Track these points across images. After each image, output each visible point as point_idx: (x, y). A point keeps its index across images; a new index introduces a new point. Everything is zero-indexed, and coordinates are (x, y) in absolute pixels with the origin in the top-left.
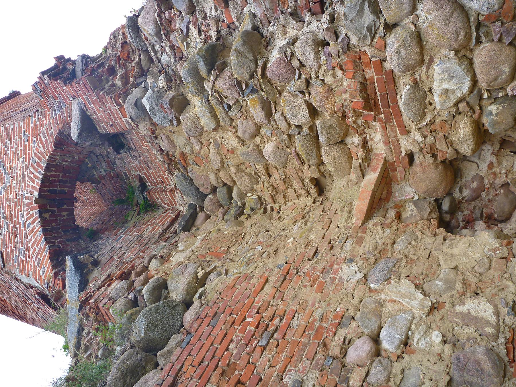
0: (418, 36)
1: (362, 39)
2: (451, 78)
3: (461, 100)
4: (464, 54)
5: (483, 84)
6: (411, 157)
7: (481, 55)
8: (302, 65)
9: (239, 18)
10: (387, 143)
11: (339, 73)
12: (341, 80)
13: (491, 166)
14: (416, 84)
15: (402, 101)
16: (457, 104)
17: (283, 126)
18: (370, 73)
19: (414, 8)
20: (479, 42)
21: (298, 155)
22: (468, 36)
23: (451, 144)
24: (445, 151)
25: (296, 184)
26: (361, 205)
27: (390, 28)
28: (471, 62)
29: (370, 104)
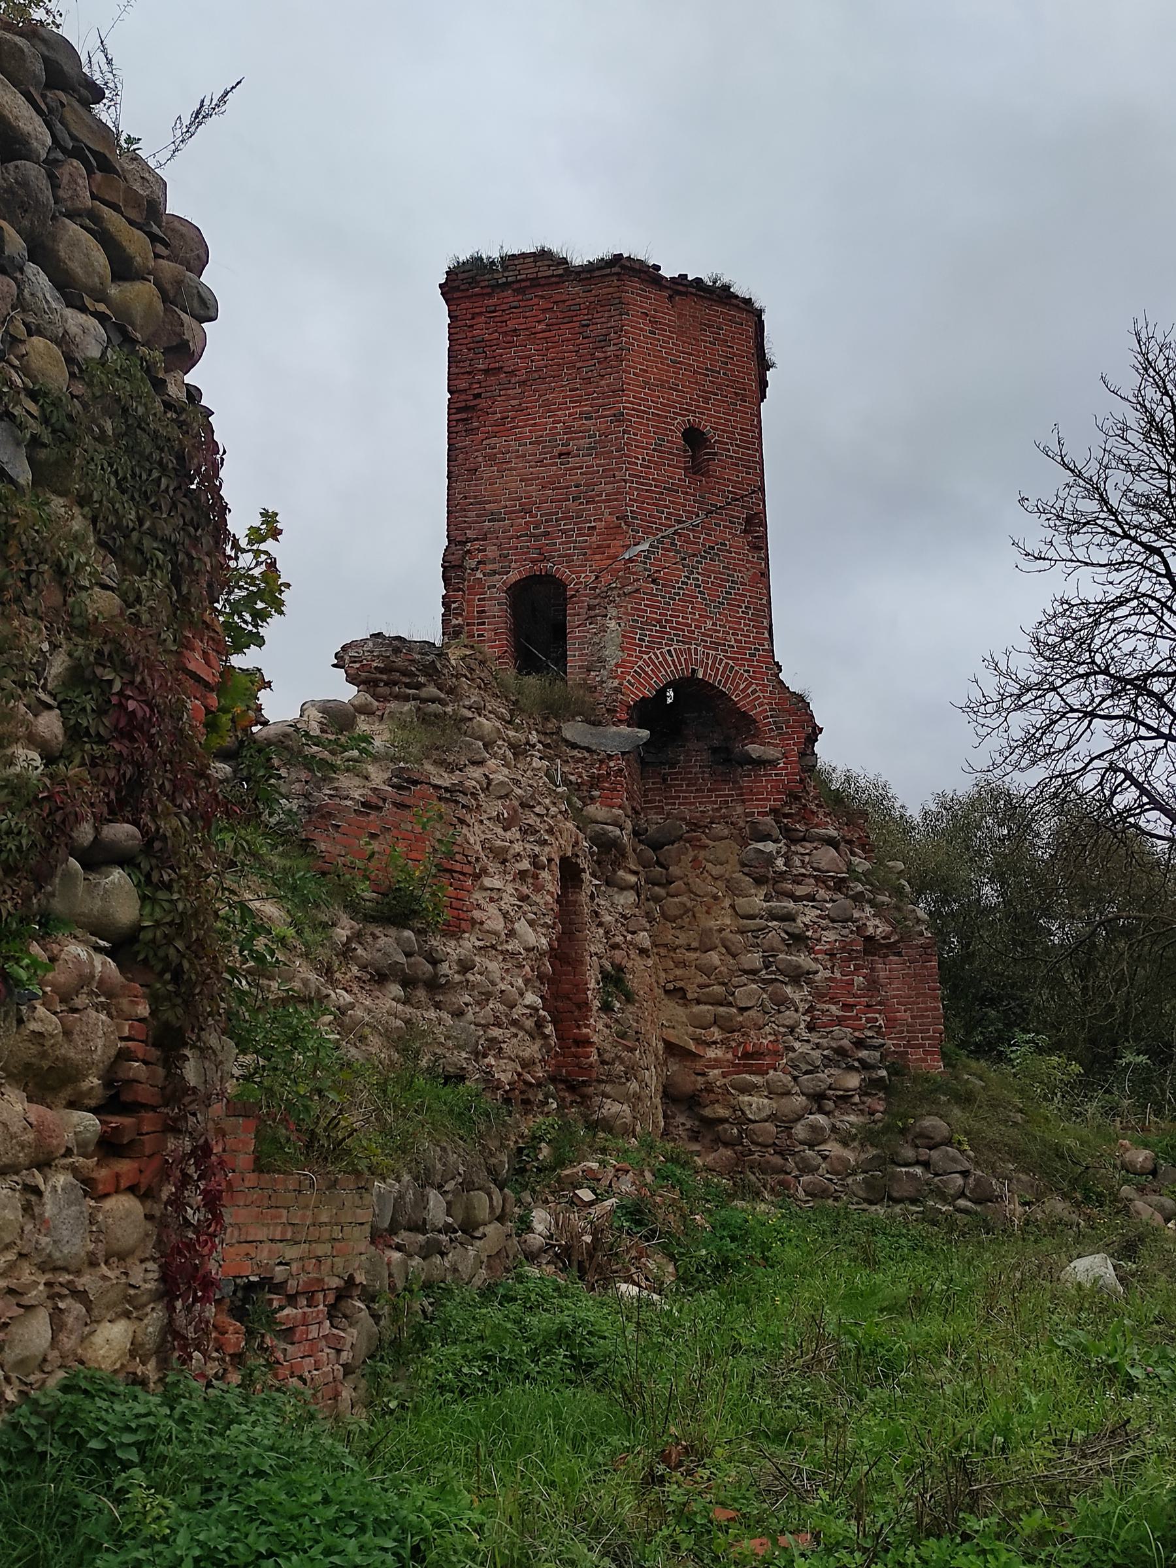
0: (788, 1093)
1: (792, 1060)
2: (759, 1109)
3: (743, 1113)
4: (772, 1117)
5: (751, 1126)
6: (704, 1074)
7: (770, 1127)
8: (779, 1012)
9: (816, 960)
10: (716, 1060)
11: (772, 1038)
12: (765, 1038)
13: (683, 1124)
14: (755, 1086)
15: (748, 1077)
16: (741, 1110)
17: (735, 980)
18: (768, 1061)
19: (803, 1094)
20: (777, 1126)
21: (709, 986)
22: (784, 1122)
23: (712, 1103)
24: (707, 1097)
25: (678, 972)
26: (672, 1036)
27: (795, 1078)
28: (766, 1121)
29: (746, 1055)
